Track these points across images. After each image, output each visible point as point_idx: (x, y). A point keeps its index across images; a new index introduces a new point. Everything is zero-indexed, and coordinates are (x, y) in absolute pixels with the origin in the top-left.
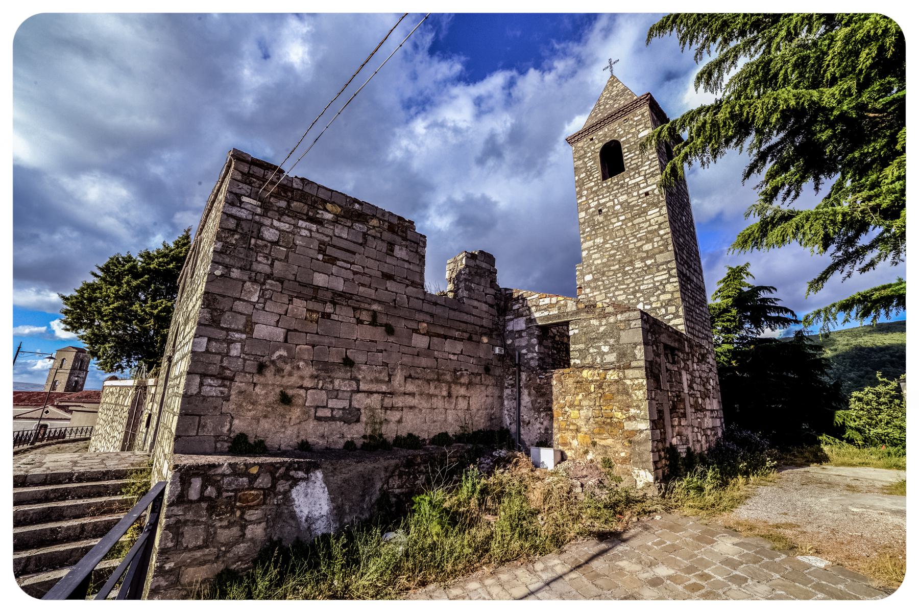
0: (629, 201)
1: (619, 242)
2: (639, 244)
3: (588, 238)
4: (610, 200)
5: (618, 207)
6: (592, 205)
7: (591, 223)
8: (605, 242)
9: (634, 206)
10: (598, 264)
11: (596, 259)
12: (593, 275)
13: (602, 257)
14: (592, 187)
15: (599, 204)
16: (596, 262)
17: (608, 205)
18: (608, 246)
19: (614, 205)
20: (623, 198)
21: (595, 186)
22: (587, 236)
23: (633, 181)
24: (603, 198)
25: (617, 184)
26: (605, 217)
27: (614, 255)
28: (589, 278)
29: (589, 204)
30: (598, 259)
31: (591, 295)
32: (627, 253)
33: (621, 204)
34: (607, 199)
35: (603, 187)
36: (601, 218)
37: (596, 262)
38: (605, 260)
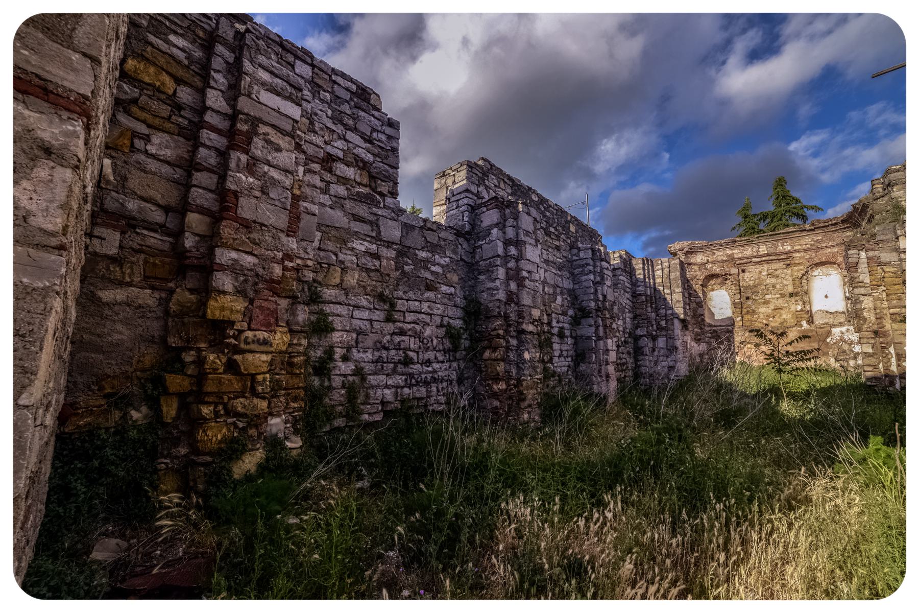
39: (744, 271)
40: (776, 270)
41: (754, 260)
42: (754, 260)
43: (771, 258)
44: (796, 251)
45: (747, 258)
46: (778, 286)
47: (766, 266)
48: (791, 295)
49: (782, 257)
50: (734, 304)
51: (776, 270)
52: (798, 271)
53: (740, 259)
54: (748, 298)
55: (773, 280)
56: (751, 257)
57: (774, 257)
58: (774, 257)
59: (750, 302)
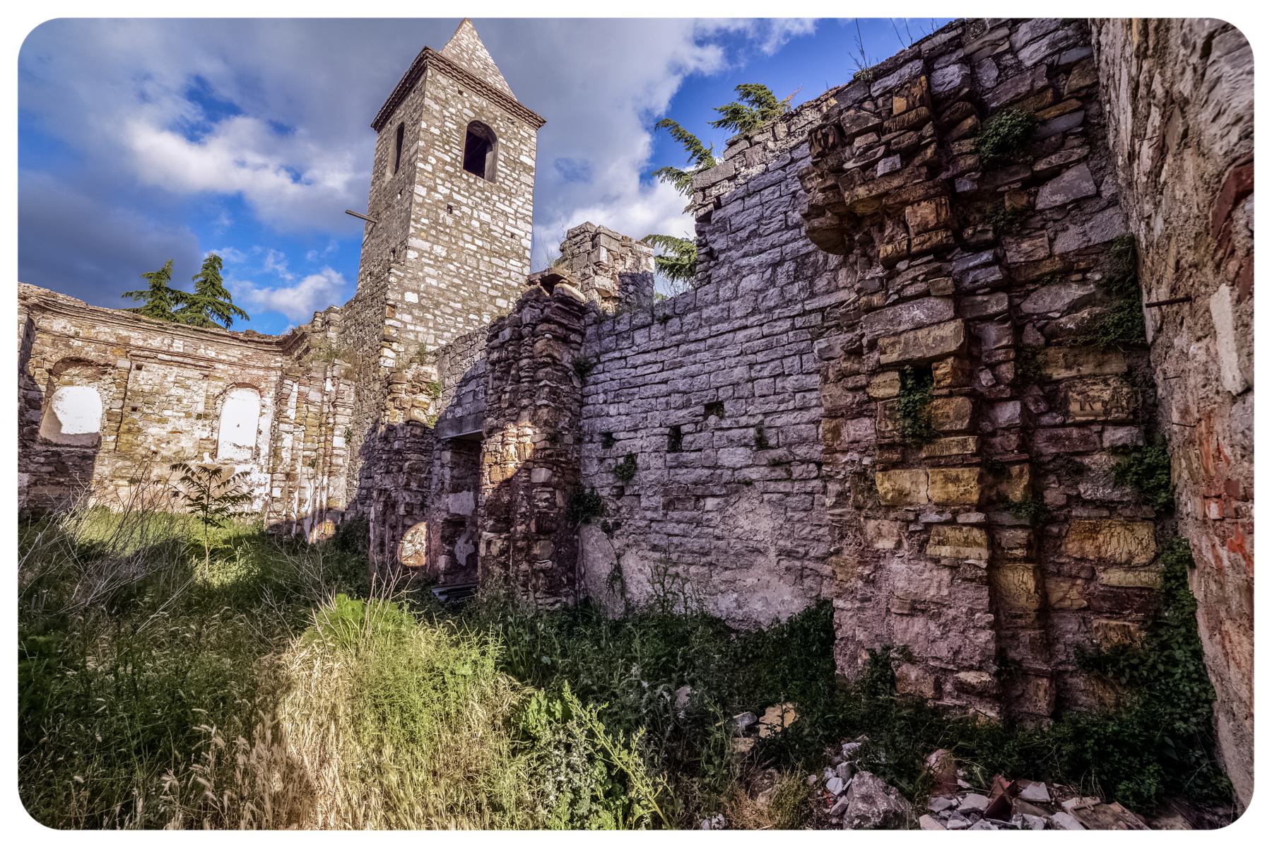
0: (492, 227)
1: (468, 272)
2: (493, 293)
3: (423, 234)
4: (467, 205)
5: (476, 224)
6: (440, 188)
7: (432, 215)
8: (448, 259)
9: (496, 238)
10: (431, 286)
11: (429, 275)
12: (421, 298)
13: (439, 278)
14: (445, 163)
15: (450, 197)
16: (428, 280)
17: (464, 209)
18: (452, 267)
19: (471, 218)
20: (486, 217)
21: (452, 165)
22: (422, 230)
23: (502, 207)
24: (458, 193)
25: (482, 190)
26: (457, 223)
27: (457, 286)
28: (411, 298)
29: (436, 184)
30: (433, 277)
31: (409, 327)
32: (476, 294)
33: (482, 223)
34: (465, 201)
35: (461, 177)
36: (449, 221)
37: (428, 280)
38: (443, 286)
39: (139, 368)
40: (188, 378)
41: (160, 356)
42: (160, 356)
43: (186, 360)
44: (220, 361)
45: (151, 350)
46: (185, 401)
47: (176, 369)
48: (199, 417)
49: (202, 363)
50: (109, 414)
51: (188, 378)
52: (215, 387)
53: (139, 348)
54: (134, 409)
55: (181, 392)
56: (158, 351)
57: (190, 361)
58: (190, 361)
59: (136, 416)
